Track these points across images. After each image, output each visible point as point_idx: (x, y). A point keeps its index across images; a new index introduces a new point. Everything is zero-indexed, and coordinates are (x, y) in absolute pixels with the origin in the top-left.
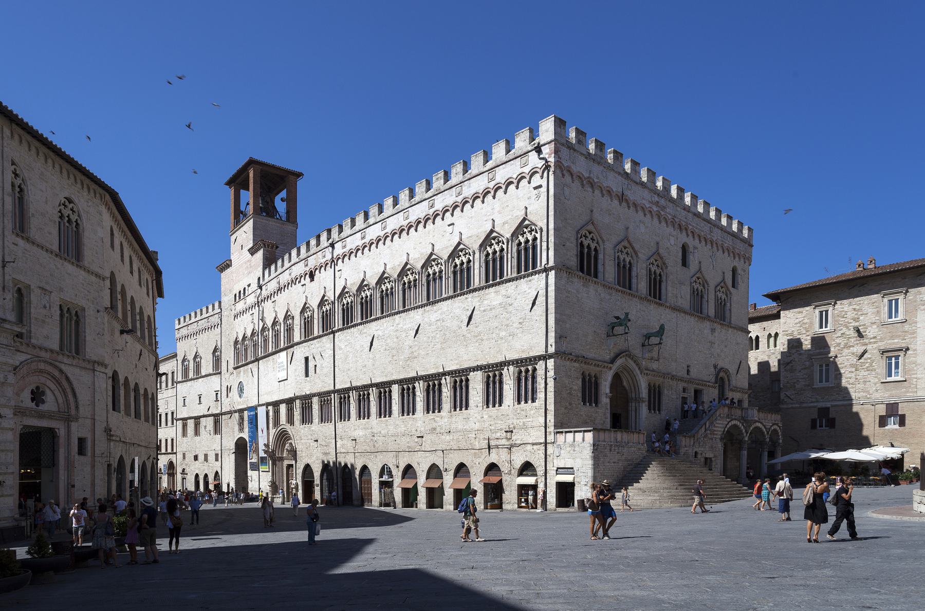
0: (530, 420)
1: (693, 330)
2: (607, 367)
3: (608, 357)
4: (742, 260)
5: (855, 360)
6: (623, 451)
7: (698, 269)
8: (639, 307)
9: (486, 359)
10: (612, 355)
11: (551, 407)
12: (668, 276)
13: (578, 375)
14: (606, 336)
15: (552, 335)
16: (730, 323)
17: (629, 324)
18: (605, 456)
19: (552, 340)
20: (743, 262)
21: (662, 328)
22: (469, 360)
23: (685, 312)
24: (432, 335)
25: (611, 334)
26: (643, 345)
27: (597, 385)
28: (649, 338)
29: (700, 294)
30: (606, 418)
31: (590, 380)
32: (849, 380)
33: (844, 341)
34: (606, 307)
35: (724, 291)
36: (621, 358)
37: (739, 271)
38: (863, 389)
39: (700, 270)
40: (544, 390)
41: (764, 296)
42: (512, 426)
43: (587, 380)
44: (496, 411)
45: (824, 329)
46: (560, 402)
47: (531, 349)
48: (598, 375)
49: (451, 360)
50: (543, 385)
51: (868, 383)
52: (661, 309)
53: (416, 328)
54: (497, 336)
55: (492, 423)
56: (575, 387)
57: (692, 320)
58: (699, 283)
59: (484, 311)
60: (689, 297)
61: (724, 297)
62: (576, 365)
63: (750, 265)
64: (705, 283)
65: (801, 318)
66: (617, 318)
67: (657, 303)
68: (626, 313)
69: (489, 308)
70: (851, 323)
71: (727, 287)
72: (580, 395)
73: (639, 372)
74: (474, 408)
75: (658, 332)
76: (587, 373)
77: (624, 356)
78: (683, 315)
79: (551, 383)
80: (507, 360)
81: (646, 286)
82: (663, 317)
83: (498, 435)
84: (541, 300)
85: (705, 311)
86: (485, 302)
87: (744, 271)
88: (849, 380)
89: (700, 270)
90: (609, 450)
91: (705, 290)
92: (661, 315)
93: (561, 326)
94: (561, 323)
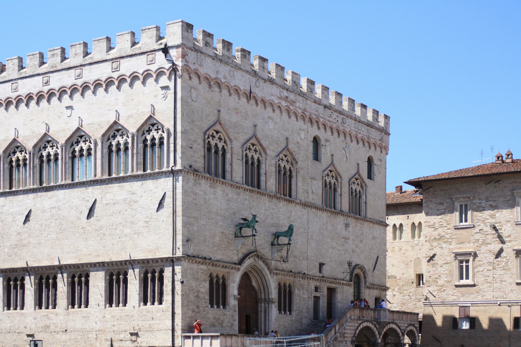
0: (156, 322)
2: (235, 268)
3: (236, 258)
4: (378, 149)
5: (492, 258)
7: (330, 162)
8: (267, 205)
9: (109, 255)
10: (241, 255)
11: (178, 310)
12: (298, 172)
13: (205, 277)
14: (233, 236)
15: (179, 238)
16: (366, 217)
17: (257, 226)
19: (179, 244)
20: (380, 152)
21: (291, 229)
22: (89, 255)
23: (316, 208)
24: (46, 223)
25: (239, 234)
26: (272, 244)
27: (225, 287)
28: (278, 237)
29: (333, 188)
31: (217, 281)
32: (487, 278)
33: (482, 237)
34: (234, 207)
35: (359, 183)
36: (249, 258)
37: (376, 161)
38: (499, 289)
39: (332, 164)
40: (171, 293)
41: (404, 182)
42: (137, 328)
43: (215, 282)
44: (120, 311)
45: (464, 223)
46: (187, 305)
47: (158, 250)
48: (226, 276)
49: (69, 253)
50: (170, 288)
51: (504, 283)
52: (291, 206)
53: (26, 213)
54: (121, 232)
55: (115, 323)
56: (203, 290)
57: (325, 215)
58: (333, 176)
59: (107, 204)
60: (320, 192)
61: (359, 189)
62: (204, 267)
63: (387, 154)
64: (338, 176)
65: (442, 209)
66: (245, 220)
67: (287, 200)
68: (253, 216)
69: (112, 202)
70: (488, 219)
71: (362, 179)
73: (268, 272)
74: (96, 306)
75: (287, 232)
77: (252, 256)
78: (314, 210)
79: (178, 287)
80: (132, 259)
81: (275, 184)
83: (122, 336)
84: (168, 201)
85: (338, 206)
86: (108, 196)
87: (381, 161)
88: (487, 278)
89: (332, 164)
91: (338, 184)
92: (291, 212)
93: (188, 229)
94: (188, 226)
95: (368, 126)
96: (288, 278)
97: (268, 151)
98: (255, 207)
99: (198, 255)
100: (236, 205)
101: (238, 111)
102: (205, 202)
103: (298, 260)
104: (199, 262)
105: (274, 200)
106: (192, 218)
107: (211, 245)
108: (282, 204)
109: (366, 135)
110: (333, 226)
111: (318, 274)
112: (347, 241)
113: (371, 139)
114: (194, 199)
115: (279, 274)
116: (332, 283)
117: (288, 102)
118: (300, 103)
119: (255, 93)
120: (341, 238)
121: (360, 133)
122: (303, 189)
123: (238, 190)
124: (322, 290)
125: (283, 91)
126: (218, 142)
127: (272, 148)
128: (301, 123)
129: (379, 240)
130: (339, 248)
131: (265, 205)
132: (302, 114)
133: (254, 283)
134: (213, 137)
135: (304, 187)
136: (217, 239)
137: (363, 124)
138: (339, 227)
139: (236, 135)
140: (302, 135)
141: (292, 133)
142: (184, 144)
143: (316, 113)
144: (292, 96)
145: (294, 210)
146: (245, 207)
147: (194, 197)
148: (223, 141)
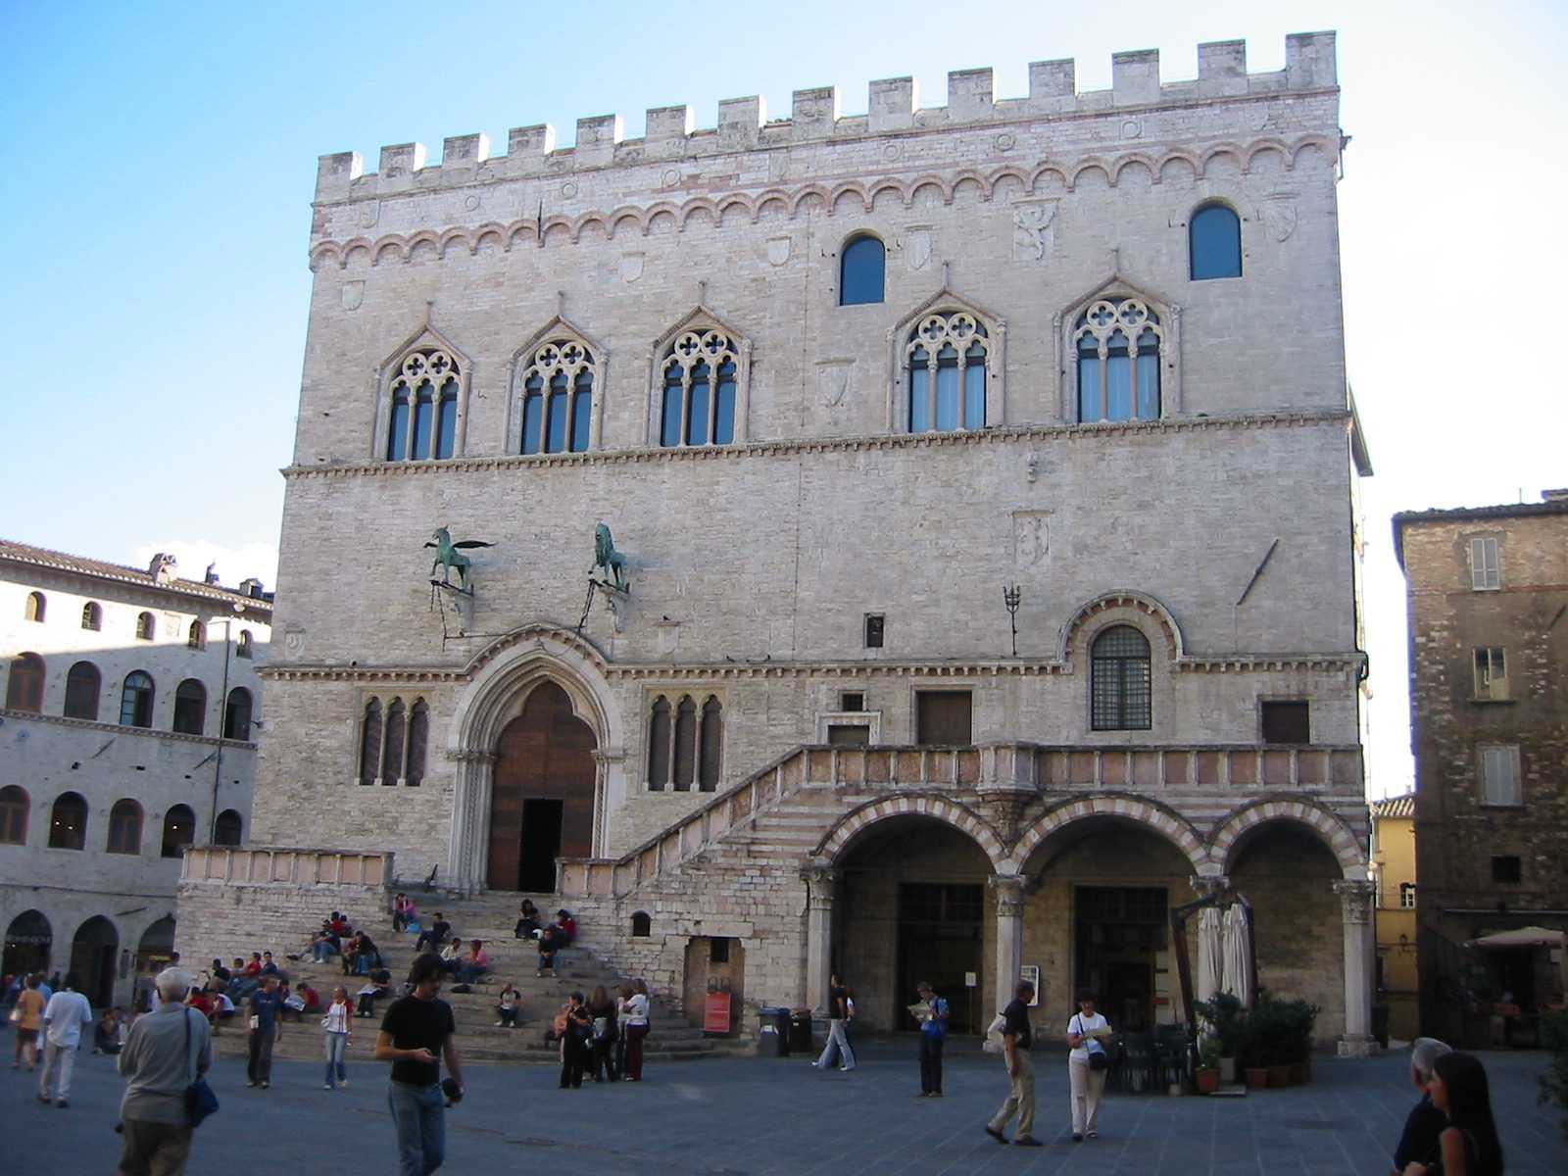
1: (899, 493)
3: (462, 648)
6: (286, 905)
13: (342, 710)
18: (219, 915)
30: (439, 817)
36: (505, 644)
46: (274, 783)
52: (706, 469)
56: (332, 743)
72: (350, 761)
76: (385, 702)
82: (721, 488)
90: (232, 901)
92: (718, 483)
93: (294, 601)
95: (1165, 109)
96: (693, 679)
97: (613, 344)
98: (546, 502)
99: (321, 657)
100: (471, 512)
101: (501, 280)
102: (358, 530)
103: (744, 620)
104: (316, 675)
105: (634, 466)
106: (308, 574)
107: (370, 630)
108: (667, 470)
109: (1154, 144)
110: (947, 484)
111: (858, 651)
112: (1047, 520)
113: (1192, 146)
114: (322, 528)
115: (639, 672)
116: (932, 671)
117: (702, 186)
118: (757, 173)
119: (557, 216)
120: (1001, 514)
121: (1116, 149)
122: (776, 406)
123: (482, 473)
124: (878, 702)
125: (680, 165)
126: (432, 375)
127: (633, 328)
128: (776, 222)
129: (1283, 482)
130: (984, 551)
131: (591, 488)
132: (770, 196)
133: (581, 710)
134: (415, 367)
135: (788, 399)
136: (394, 610)
137: (1131, 113)
138: (985, 483)
139: (487, 338)
140: (780, 252)
141: (729, 260)
142: (308, 413)
143: (835, 172)
144: (719, 166)
145: (727, 475)
146: (507, 509)
147: (323, 523)
148: (449, 367)
